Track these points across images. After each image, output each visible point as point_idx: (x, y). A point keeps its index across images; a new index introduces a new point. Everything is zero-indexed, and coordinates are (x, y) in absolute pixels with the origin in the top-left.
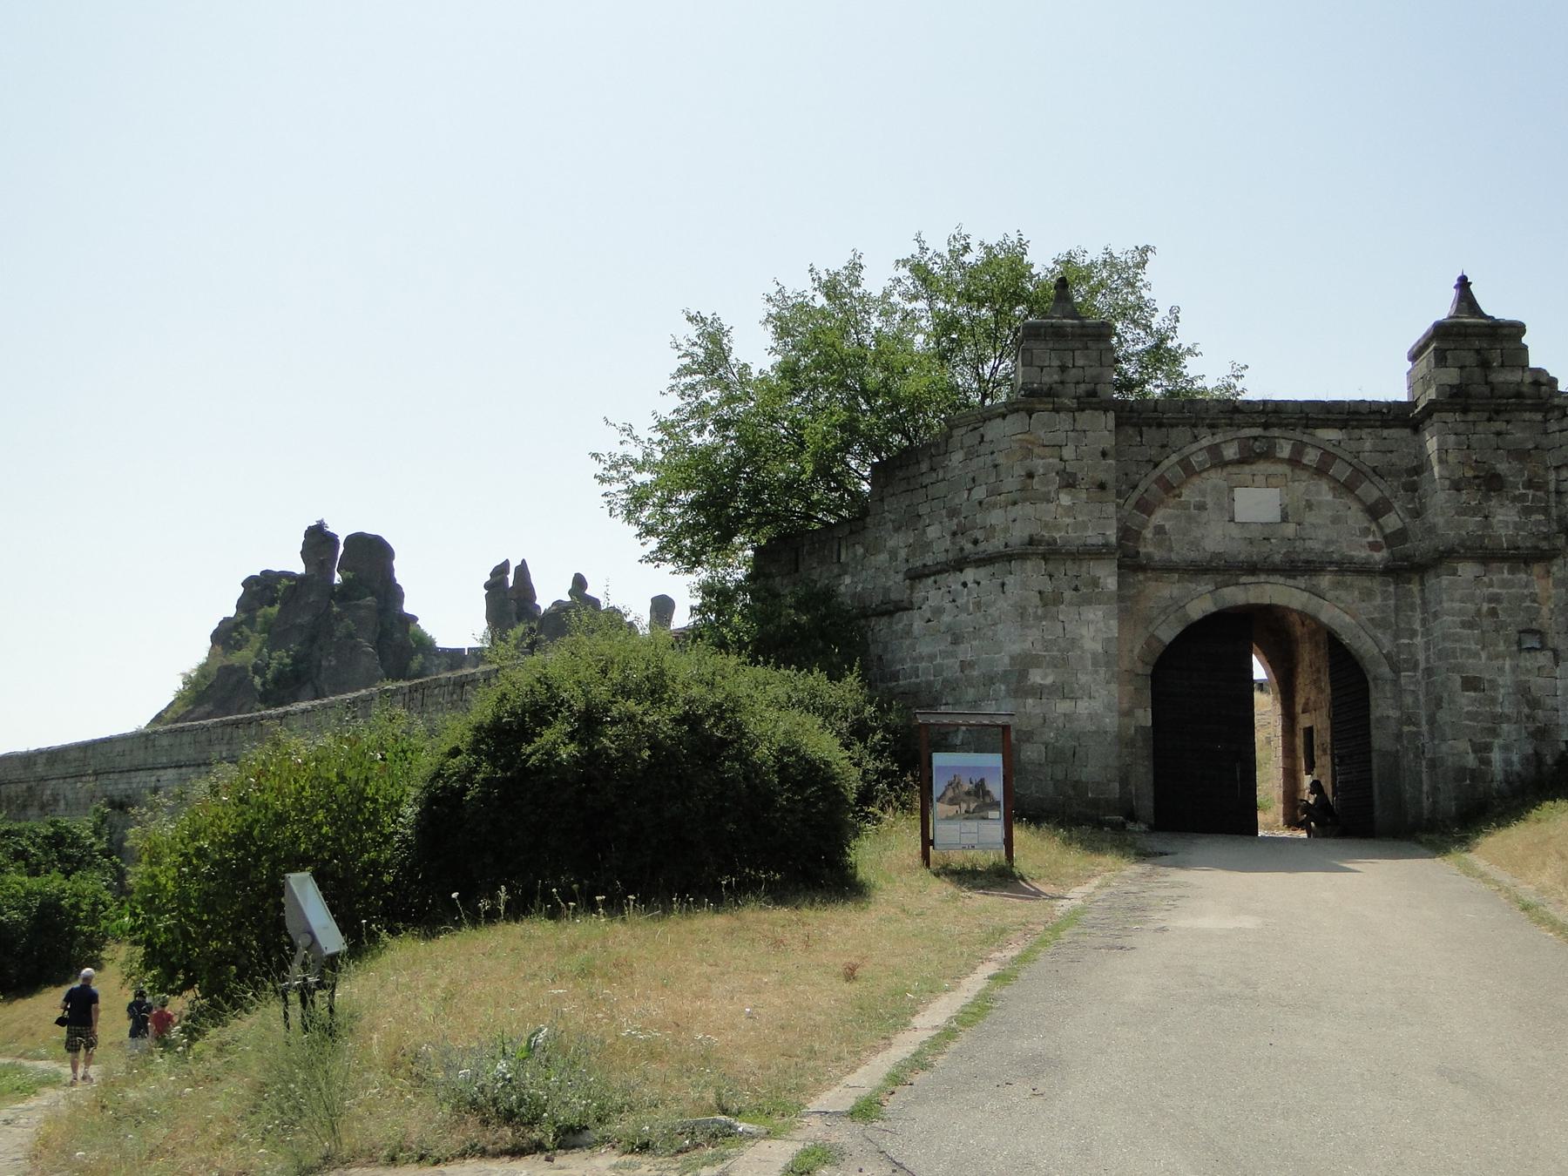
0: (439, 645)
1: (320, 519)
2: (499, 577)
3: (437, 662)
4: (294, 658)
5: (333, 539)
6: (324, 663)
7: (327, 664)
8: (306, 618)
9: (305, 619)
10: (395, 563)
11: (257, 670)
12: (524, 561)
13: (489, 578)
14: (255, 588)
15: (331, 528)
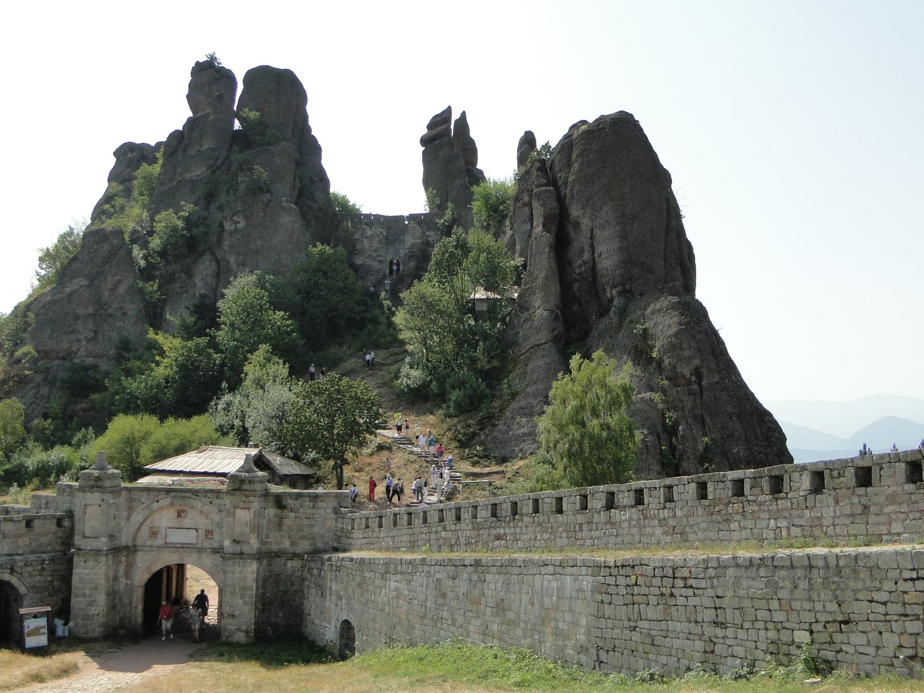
0: (365, 210)
1: (211, 53)
2: (440, 128)
3: (369, 232)
4: (187, 220)
5: (227, 77)
6: (228, 226)
7: (233, 228)
8: (199, 173)
9: (199, 171)
10: (310, 108)
11: (136, 238)
12: (464, 114)
13: (425, 131)
14: (130, 155)
15: (226, 62)
